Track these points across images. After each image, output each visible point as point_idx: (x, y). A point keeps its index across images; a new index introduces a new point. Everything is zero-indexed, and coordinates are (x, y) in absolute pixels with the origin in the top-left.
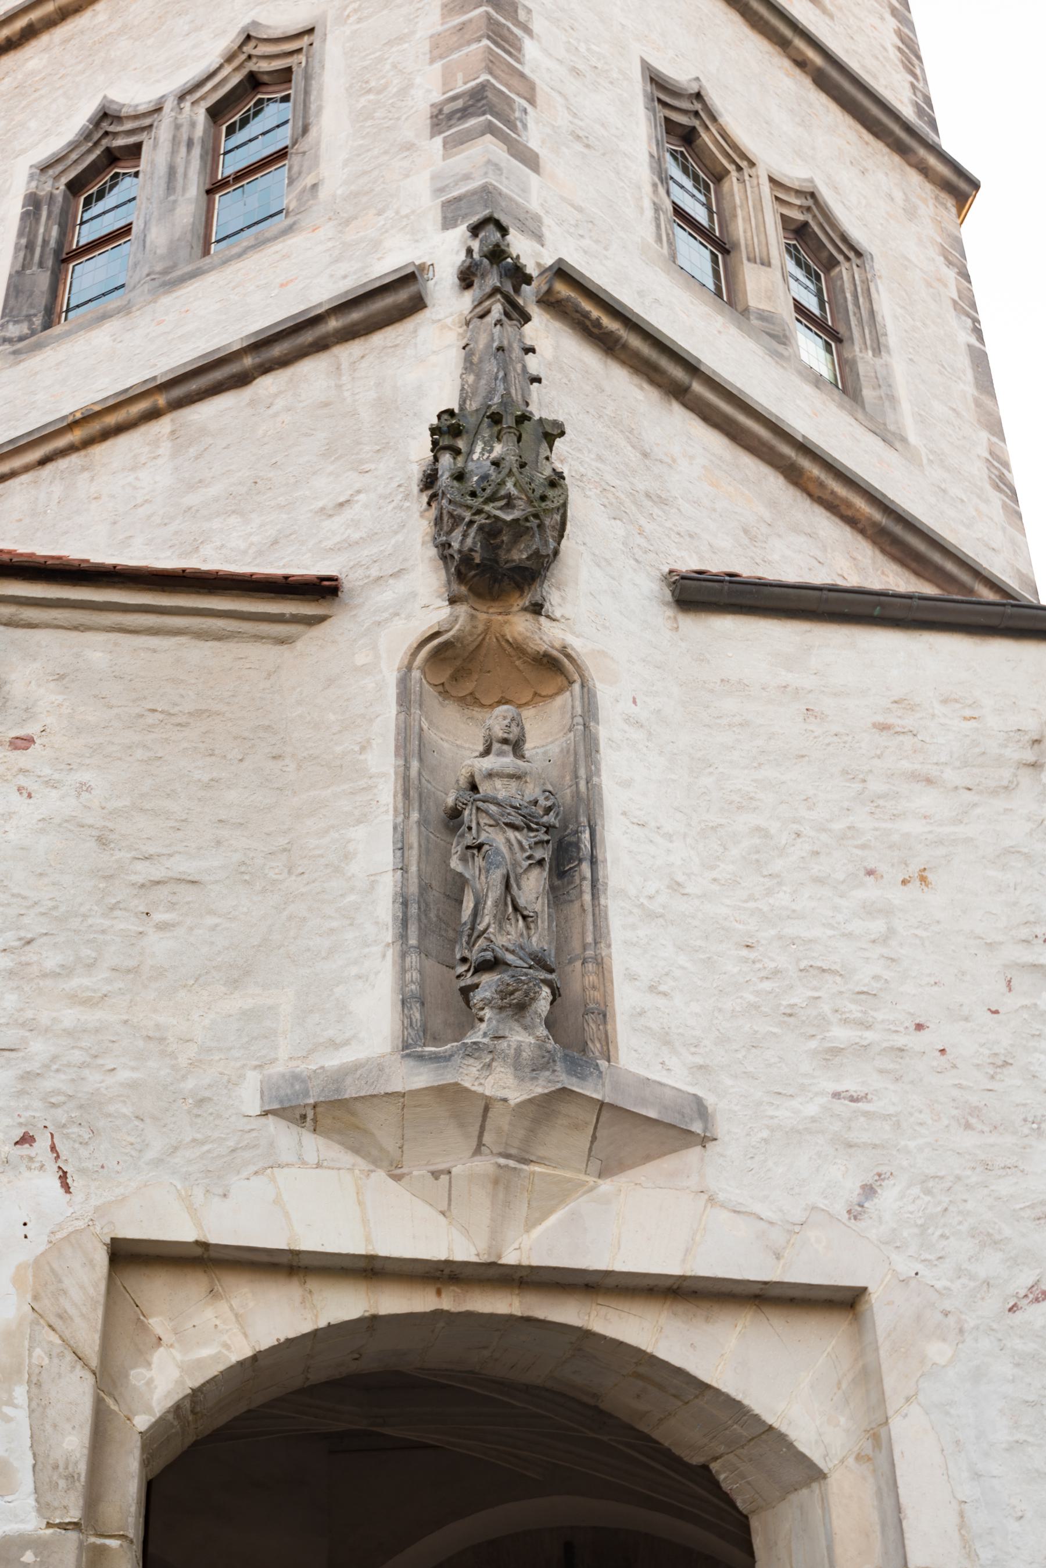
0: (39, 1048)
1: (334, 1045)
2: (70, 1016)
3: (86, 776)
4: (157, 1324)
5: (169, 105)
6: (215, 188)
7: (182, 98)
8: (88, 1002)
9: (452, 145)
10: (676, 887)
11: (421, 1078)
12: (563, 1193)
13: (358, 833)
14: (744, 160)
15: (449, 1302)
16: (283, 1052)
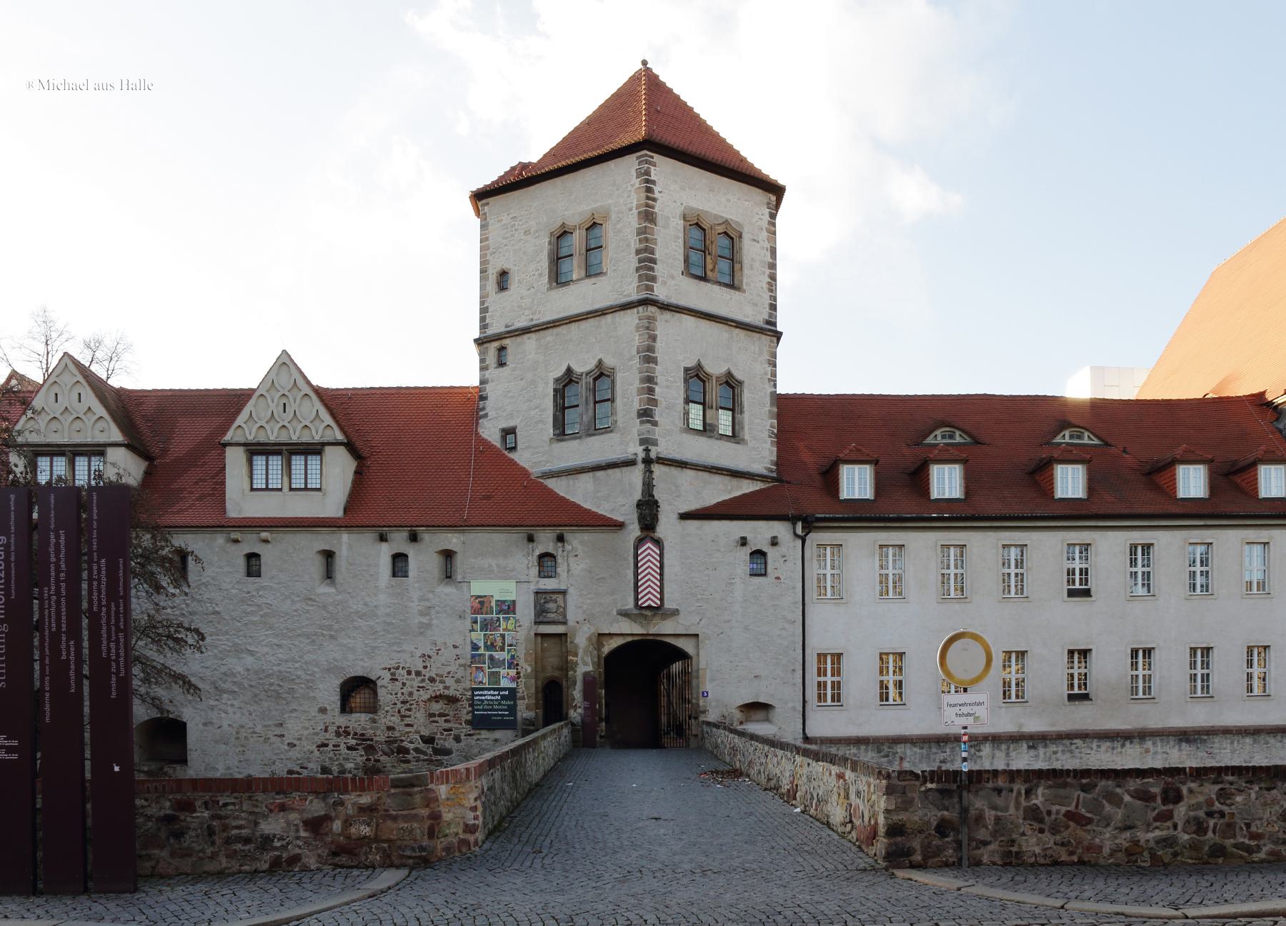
0: (585, 607)
1: (626, 605)
2: (589, 601)
3: (587, 561)
4: (605, 643)
5: (584, 376)
6: (596, 402)
7: (587, 375)
8: (591, 599)
9: (642, 422)
10: (676, 575)
11: (637, 612)
12: (658, 624)
13: (628, 571)
14: (709, 376)
15: (643, 638)
16: (619, 605)
